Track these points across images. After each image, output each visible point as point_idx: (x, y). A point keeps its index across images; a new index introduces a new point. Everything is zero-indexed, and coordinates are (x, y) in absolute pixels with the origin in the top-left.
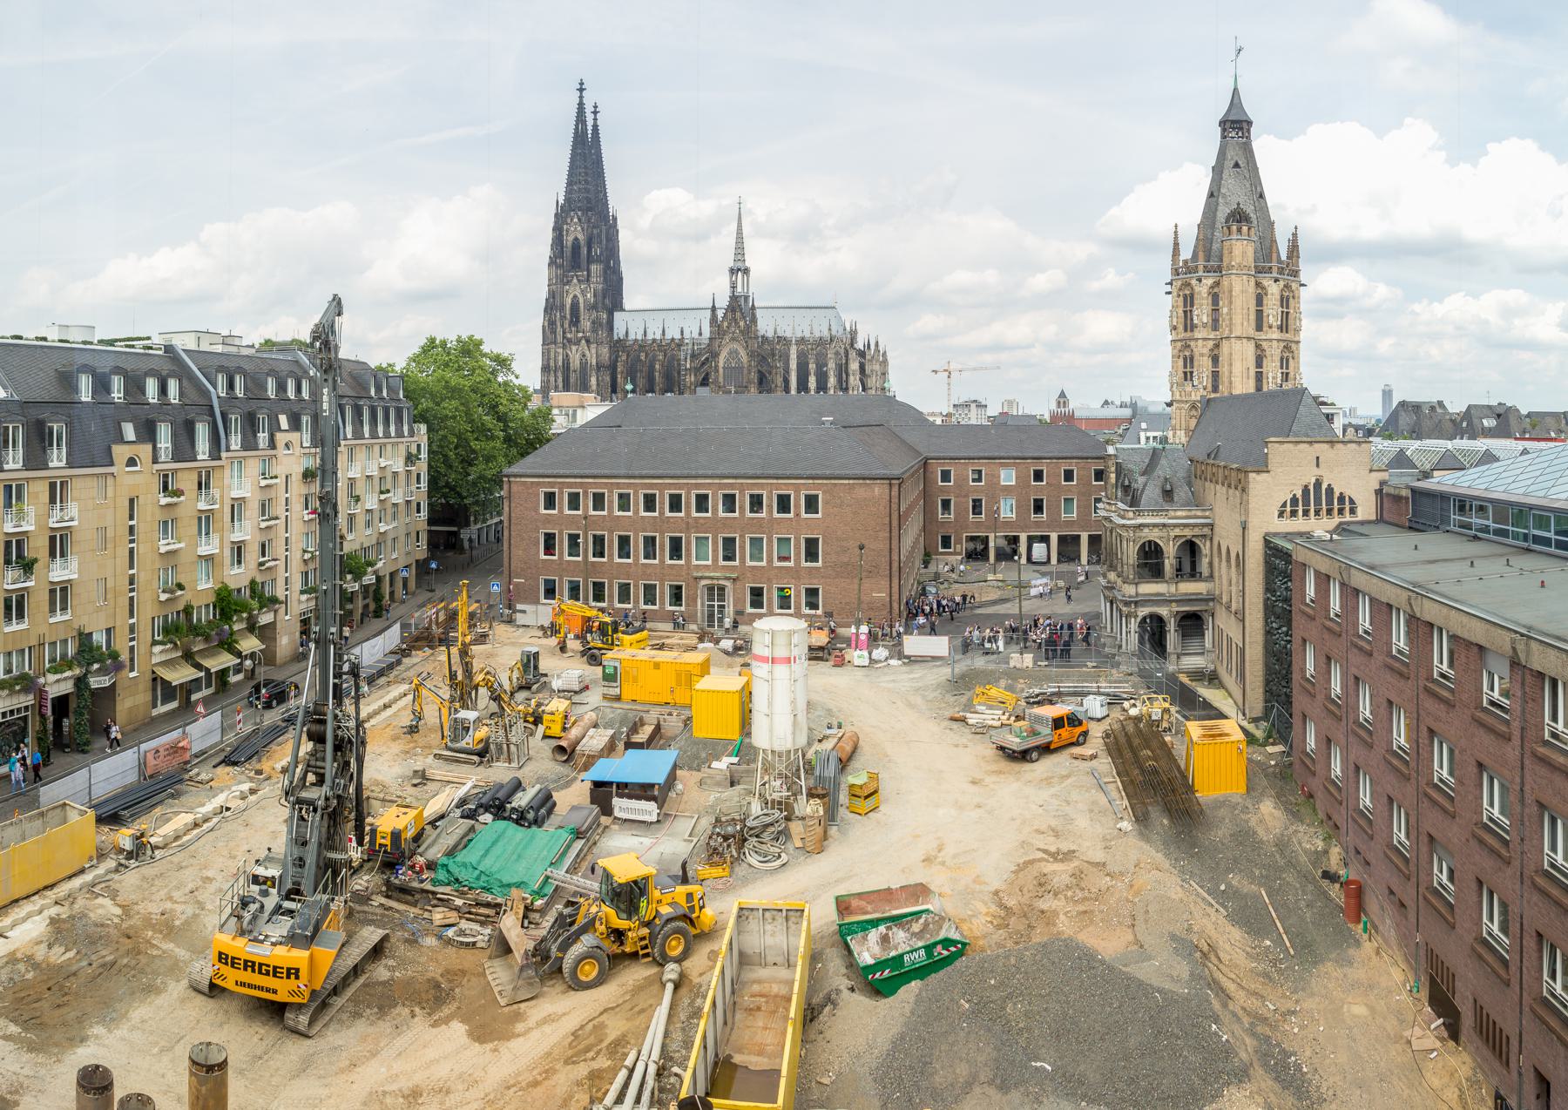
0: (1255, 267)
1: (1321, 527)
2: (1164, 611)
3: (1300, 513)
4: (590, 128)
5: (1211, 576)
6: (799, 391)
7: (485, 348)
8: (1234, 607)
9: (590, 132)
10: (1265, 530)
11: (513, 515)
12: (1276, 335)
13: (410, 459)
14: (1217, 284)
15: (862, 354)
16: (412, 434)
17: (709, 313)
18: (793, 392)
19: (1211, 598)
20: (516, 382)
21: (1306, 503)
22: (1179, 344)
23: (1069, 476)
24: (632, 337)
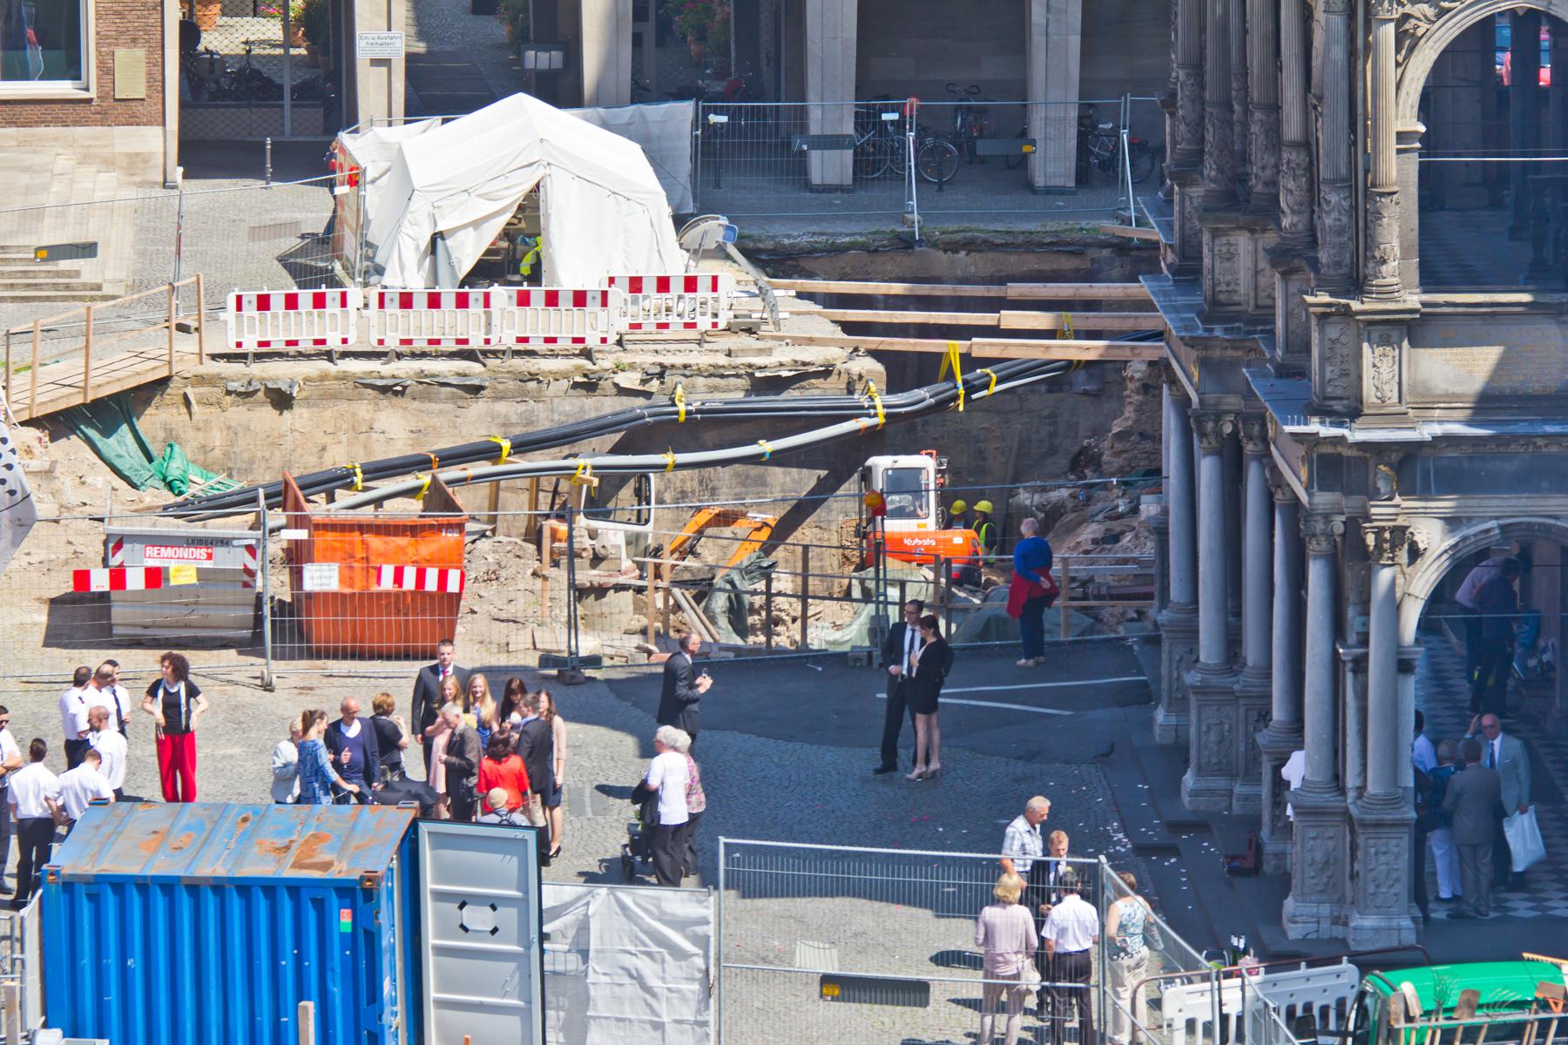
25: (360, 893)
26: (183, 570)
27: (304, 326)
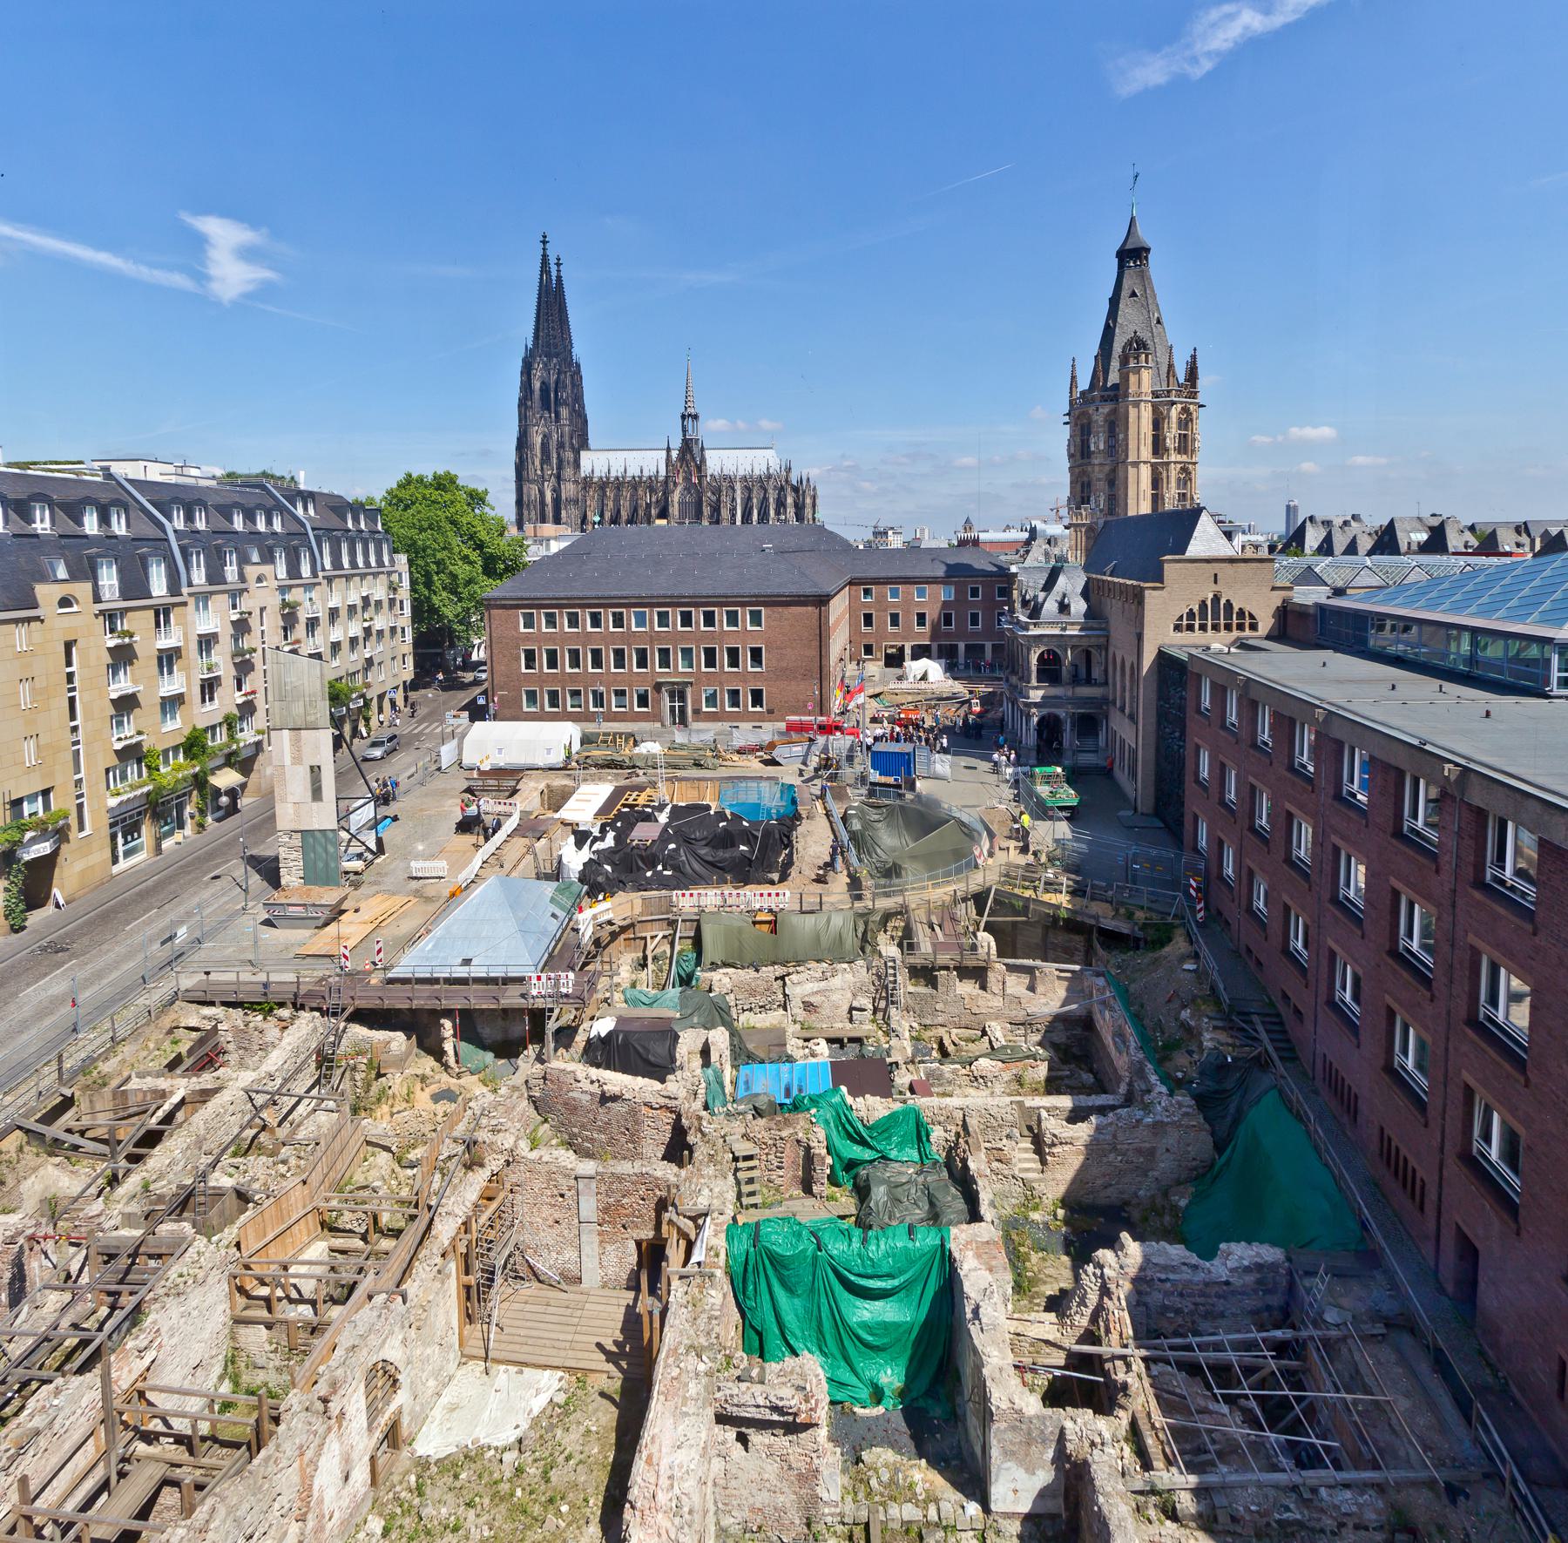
0: (1153, 392)
1: (1218, 643)
2: (1061, 713)
3: (1197, 627)
5: (1106, 683)
7: (460, 482)
8: (1127, 711)
10: (1160, 642)
12: (1174, 457)
13: (393, 588)
14: (1114, 411)
15: (796, 490)
16: (392, 562)
18: (738, 522)
19: (1105, 702)
20: (492, 514)
21: (1203, 615)
22: (1077, 470)
23: (975, 593)
24: (597, 474)
25: (908, 754)
26: (886, 714)
27: (899, 686)
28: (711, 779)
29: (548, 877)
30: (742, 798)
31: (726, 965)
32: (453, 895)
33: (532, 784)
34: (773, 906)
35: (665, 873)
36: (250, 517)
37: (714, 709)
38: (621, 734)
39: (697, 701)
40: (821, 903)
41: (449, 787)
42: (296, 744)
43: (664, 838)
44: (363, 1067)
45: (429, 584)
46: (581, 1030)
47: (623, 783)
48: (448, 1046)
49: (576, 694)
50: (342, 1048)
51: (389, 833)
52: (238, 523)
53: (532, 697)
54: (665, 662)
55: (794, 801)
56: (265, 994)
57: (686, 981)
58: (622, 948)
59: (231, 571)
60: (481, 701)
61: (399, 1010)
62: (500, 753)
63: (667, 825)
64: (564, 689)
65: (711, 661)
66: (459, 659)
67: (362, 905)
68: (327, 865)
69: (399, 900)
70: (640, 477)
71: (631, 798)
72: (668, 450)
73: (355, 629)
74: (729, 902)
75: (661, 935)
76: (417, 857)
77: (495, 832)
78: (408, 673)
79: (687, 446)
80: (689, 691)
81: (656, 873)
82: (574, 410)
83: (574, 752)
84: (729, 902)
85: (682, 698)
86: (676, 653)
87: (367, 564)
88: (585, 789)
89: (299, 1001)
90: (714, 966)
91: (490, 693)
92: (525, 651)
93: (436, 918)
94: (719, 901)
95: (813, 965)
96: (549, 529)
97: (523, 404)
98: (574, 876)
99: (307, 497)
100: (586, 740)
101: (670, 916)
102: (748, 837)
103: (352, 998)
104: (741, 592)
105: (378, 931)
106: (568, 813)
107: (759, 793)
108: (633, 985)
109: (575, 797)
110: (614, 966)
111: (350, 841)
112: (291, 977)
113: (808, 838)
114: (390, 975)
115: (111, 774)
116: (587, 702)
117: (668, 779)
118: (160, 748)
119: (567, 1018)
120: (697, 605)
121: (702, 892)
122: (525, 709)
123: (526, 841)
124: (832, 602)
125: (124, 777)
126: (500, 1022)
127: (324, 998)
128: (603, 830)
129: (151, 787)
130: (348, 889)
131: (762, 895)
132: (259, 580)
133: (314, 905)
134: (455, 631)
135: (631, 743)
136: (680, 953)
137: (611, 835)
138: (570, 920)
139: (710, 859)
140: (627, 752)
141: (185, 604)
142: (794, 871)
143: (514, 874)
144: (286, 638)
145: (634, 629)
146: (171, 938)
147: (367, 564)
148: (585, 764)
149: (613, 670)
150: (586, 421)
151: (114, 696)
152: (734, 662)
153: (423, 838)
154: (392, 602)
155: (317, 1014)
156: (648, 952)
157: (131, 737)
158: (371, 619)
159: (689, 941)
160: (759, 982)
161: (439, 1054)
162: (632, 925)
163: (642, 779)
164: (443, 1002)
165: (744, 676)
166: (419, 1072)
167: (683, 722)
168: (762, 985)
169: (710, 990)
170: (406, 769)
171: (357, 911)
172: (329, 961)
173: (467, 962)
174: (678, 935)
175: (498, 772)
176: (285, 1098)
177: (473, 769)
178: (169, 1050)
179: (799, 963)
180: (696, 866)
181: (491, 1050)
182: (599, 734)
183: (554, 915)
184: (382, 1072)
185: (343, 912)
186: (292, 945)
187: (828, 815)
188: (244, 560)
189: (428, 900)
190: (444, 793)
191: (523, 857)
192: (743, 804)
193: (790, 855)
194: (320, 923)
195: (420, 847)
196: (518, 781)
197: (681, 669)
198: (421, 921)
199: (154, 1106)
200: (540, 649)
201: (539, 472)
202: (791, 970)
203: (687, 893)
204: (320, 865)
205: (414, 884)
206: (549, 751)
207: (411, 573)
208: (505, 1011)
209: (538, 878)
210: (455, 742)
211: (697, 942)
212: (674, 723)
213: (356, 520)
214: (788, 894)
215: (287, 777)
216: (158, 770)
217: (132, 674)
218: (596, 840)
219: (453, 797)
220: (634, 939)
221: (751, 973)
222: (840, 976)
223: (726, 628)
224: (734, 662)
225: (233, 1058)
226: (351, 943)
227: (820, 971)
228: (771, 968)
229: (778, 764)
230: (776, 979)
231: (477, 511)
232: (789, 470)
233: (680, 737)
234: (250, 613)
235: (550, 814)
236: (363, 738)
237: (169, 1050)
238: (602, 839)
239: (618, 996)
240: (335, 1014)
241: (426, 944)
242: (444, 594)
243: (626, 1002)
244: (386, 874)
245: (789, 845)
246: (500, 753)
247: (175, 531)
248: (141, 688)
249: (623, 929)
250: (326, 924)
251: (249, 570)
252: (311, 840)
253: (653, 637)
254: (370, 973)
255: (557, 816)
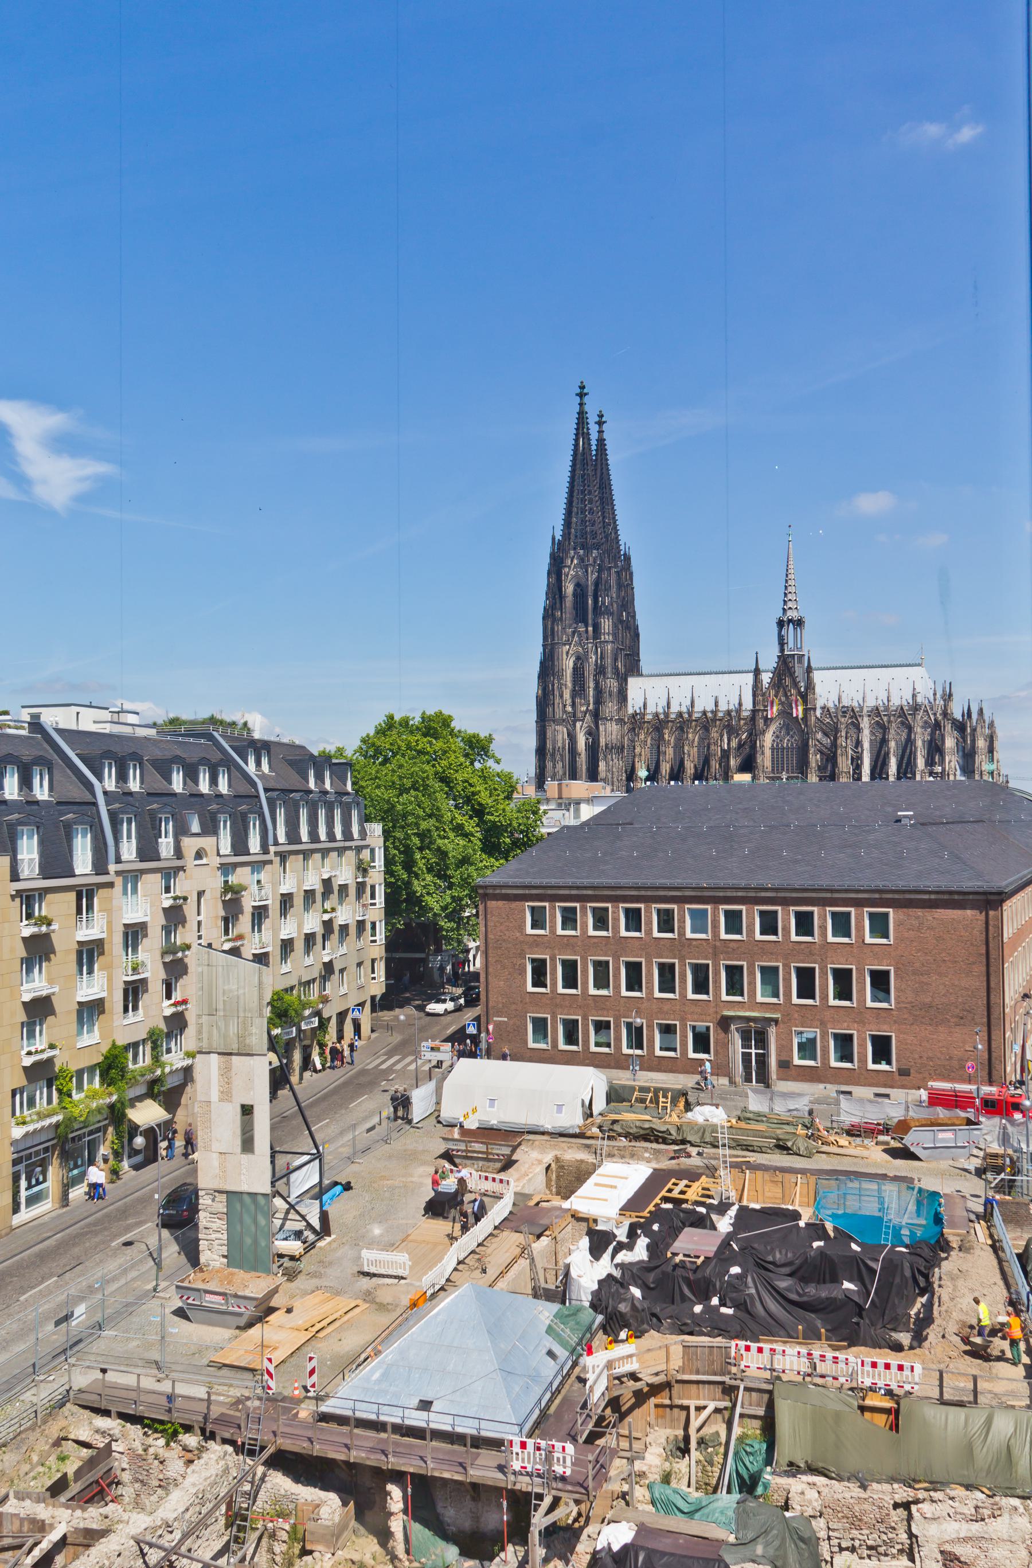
4: (594, 442)
6: (873, 777)
7: (456, 725)
9: (594, 447)
11: (491, 936)
13: (363, 869)
15: (960, 727)
17: (750, 677)
18: (866, 777)
20: (498, 768)
28: (803, 1172)
29: (549, 1296)
30: (852, 1205)
31: (812, 1470)
32: (414, 1305)
33: (535, 1155)
34: (894, 1386)
35: (724, 1310)
36: (191, 775)
37: (811, 1063)
38: (665, 1091)
39: (784, 1048)
40: (975, 1392)
41: (420, 1148)
42: (226, 1072)
43: (724, 1254)
44: (284, 1536)
45: (409, 865)
46: (584, 1536)
47: (666, 1164)
48: (396, 1525)
49: (601, 1027)
50: (259, 1503)
51: (339, 1207)
52: (178, 783)
53: (540, 1026)
54: (735, 986)
55: (938, 1220)
56: (169, 1411)
57: (748, 1485)
58: (652, 1419)
59: (166, 845)
60: (472, 1030)
61: (334, 1460)
62: (492, 1105)
63: (730, 1237)
64: (585, 1018)
65: (806, 989)
66: (449, 968)
67: (297, 1304)
68: (256, 1242)
69: (345, 1302)
70: (715, 713)
71: (677, 1189)
72: (757, 672)
73: (312, 923)
74: (821, 1368)
75: (711, 1406)
76: (371, 1244)
77: (478, 1219)
78: (377, 985)
79: (785, 666)
80: (772, 1032)
81: (709, 1309)
82: (621, 621)
83: (595, 1112)
84: (821, 1368)
85: (762, 1041)
86: (752, 974)
87: (331, 836)
88: (610, 1168)
89: (209, 1427)
90: (793, 1469)
91: (483, 1020)
92: (533, 961)
93: (387, 1335)
94: (804, 1366)
95: (959, 1492)
96: (579, 788)
97: (549, 615)
98: (586, 1299)
99: (261, 748)
100: (615, 1096)
101: (726, 1379)
102: (859, 1270)
103: (274, 1433)
104: (856, 884)
105: (313, 1343)
106: (581, 1202)
107: (881, 1200)
108: (666, 1479)
109: (593, 1179)
110: (637, 1446)
111: (287, 1212)
112: (201, 1392)
113: (960, 1283)
114: (324, 1408)
115: (18, 1097)
116: (618, 1039)
117: (734, 1166)
118: (73, 1068)
119: (566, 1512)
120: (785, 902)
121: (779, 1347)
122: (531, 1045)
123: (517, 1238)
124: (1007, 906)
125: (31, 1103)
126: (468, 1504)
127: (239, 1427)
128: (632, 1234)
129: (60, 1117)
130: (280, 1279)
131: (874, 1365)
132: (199, 855)
133: (236, 1296)
134: (442, 928)
135: (681, 1104)
136: (741, 1439)
137: (642, 1242)
138: (575, 1364)
139: (793, 1297)
140: (675, 1118)
141: (111, 885)
142: (932, 1334)
143: (501, 1284)
144: (226, 932)
145: (689, 935)
146: (67, 1318)
147: (331, 836)
148: (611, 1131)
149: (657, 994)
150: (637, 635)
151: (27, 998)
152: (844, 991)
153: (381, 1219)
154: (361, 887)
155: (230, 1449)
156: (692, 1431)
157: (42, 1051)
158: (333, 910)
159: (757, 1424)
160: (866, 1506)
161: (384, 1536)
162: (667, 1385)
163: (695, 1161)
164: (391, 1459)
165: (861, 1015)
166: (356, 1557)
167: (764, 1078)
168: (872, 1514)
169: (786, 1507)
170: (366, 1119)
171: (289, 1311)
172: (248, 1375)
173: (425, 1405)
174: (738, 1410)
175: (488, 1133)
176: (185, 1561)
177: (453, 1126)
178: (54, 1468)
179: (936, 1485)
180: (773, 1306)
181: (456, 1543)
182: (632, 1089)
183: (551, 1354)
184: (308, 1547)
185: (272, 1310)
186: (207, 1348)
187: (996, 1247)
188: (182, 831)
189: (382, 1307)
190: (411, 1157)
191: (514, 1261)
192: (854, 1216)
193: (929, 1307)
194: (242, 1322)
195: (377, 1231)
196: (514, 1149)
197: (760, 999)
198: (370, 1337)
199: (30, 1542)
200: (553, 959)
201: (569, 709)
202: (921, 1495)
203: (754, 1346)
204: (248, 1241)
205: (365, 1283)
206: (560, 1107)
207: (386, 849)
208: (475, 1486)
209: (536, 1296)
210: (432, 1085)
211: (769, 1425)
212: (748, 1079)
213: (319, 778)
214: (918, 1368)
215: (214, 1117)
216: (70, 1096)
217: (48, 973)
218: (620, 1247)
219: (424, 1163)
220: (671, 1407)
221: (856, 1491)
222: (1006, 1516)
223: (831, 939)
224: (844, 991)
225: (127, 1492)
226: (278, 1356)
227: (971, 1504)
228: (886, 1487)
229: (914, 1157)
230: (896, 1506)
231: (477, 765)
232: (948, 697)
233: (756, 1102)
234: (185, 899)
235: (557, 1202)
236: (315, 1071)
237: (54, 1468)
238: (630, 1246)
239: (640, 1493)
240: (251, 1453)
241: (373, 1371)
242: (429, 878)
243: (653, 1503)
244: (331, 1263)
245: (927, 1289)
246: (492, 1105)
247: (105, 793)
248: (56, 989)
249: (655, 1389)
250: (250, 1325)
251: (189, 845)
252: (238, 1206)
253: (718, 948)
254: (299, 1401)
255: (566, 1205)
